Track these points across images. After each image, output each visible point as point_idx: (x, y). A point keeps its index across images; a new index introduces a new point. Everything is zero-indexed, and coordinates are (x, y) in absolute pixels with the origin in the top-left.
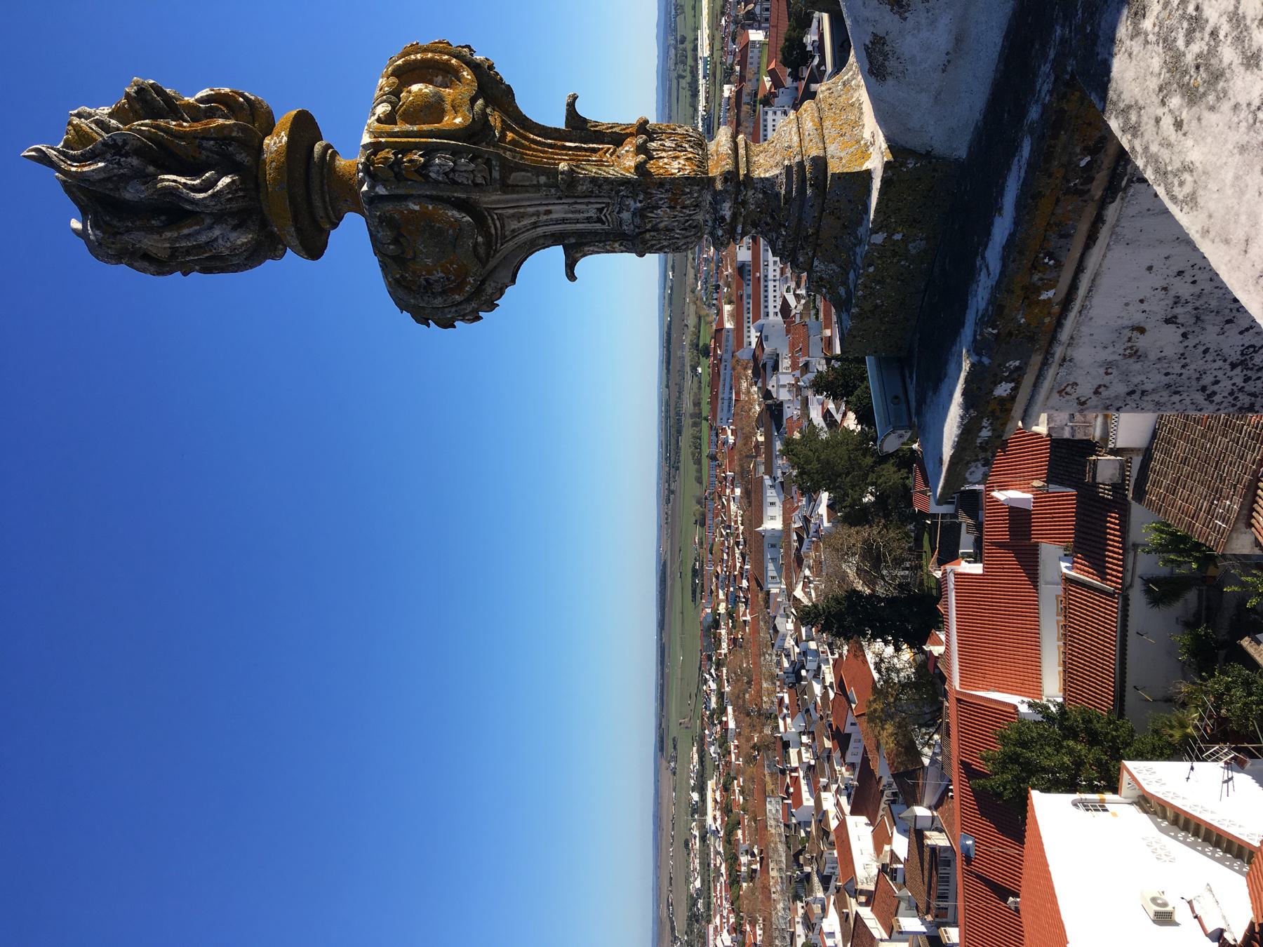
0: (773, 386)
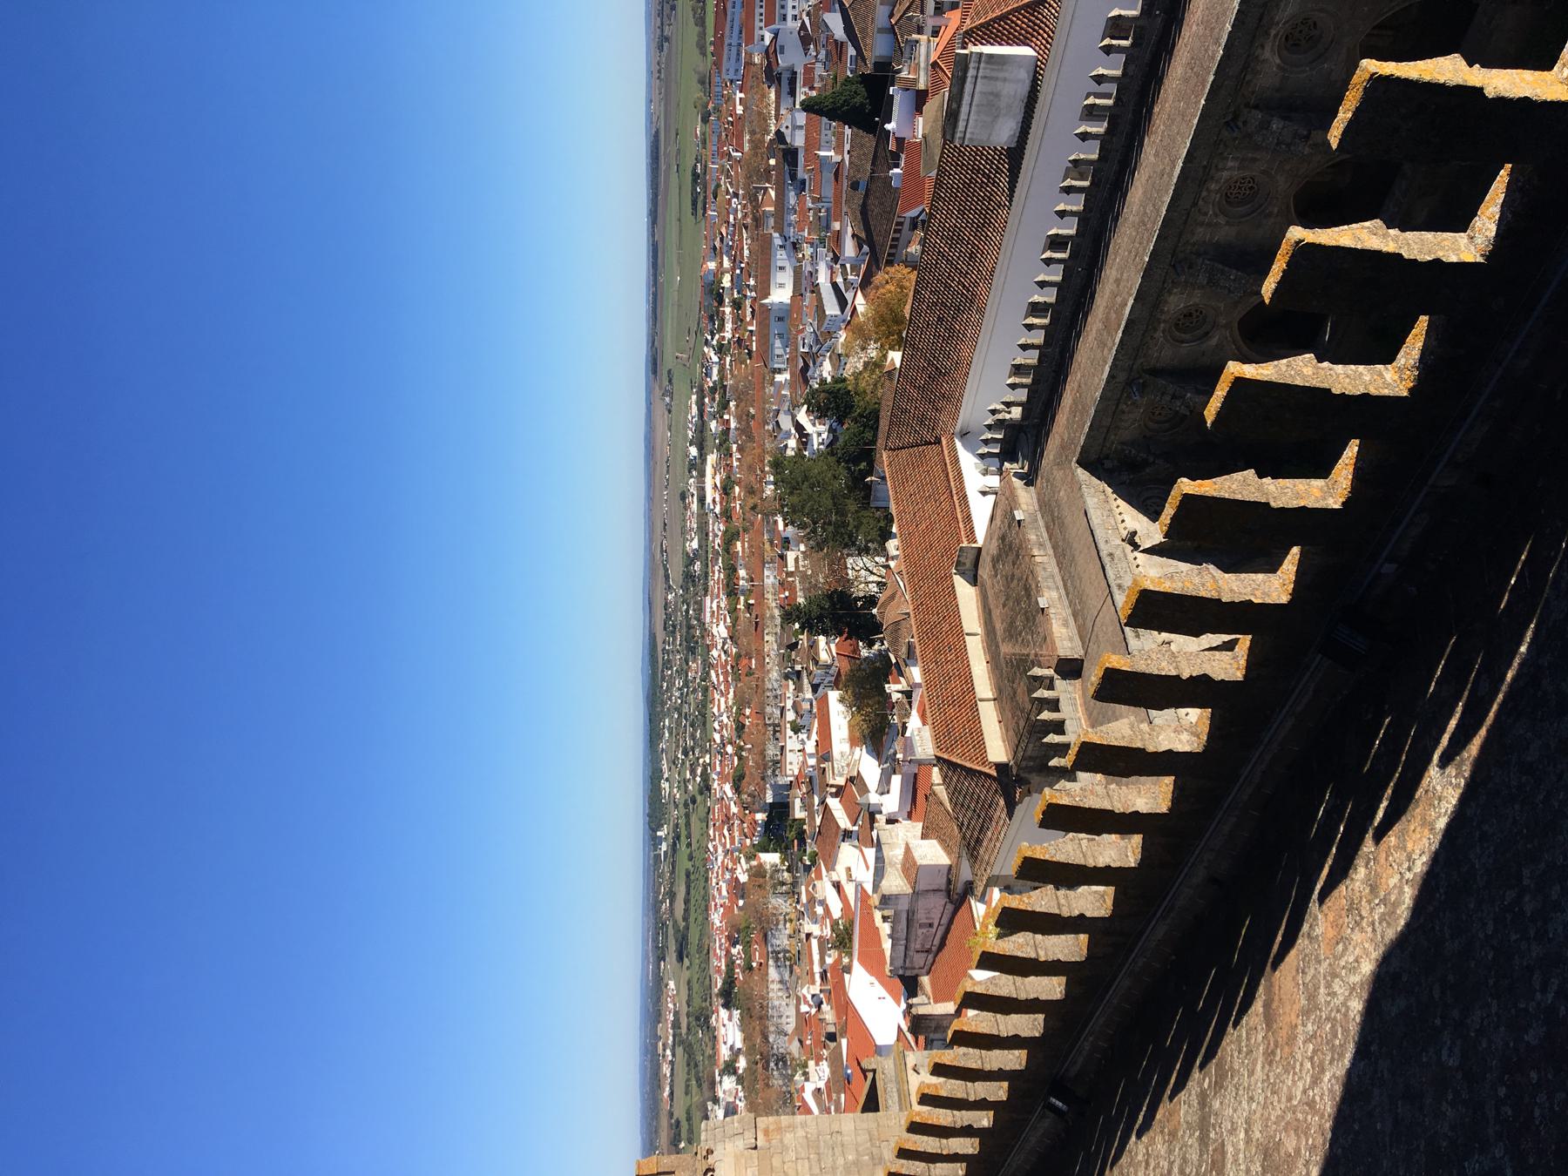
0: (787, 127)
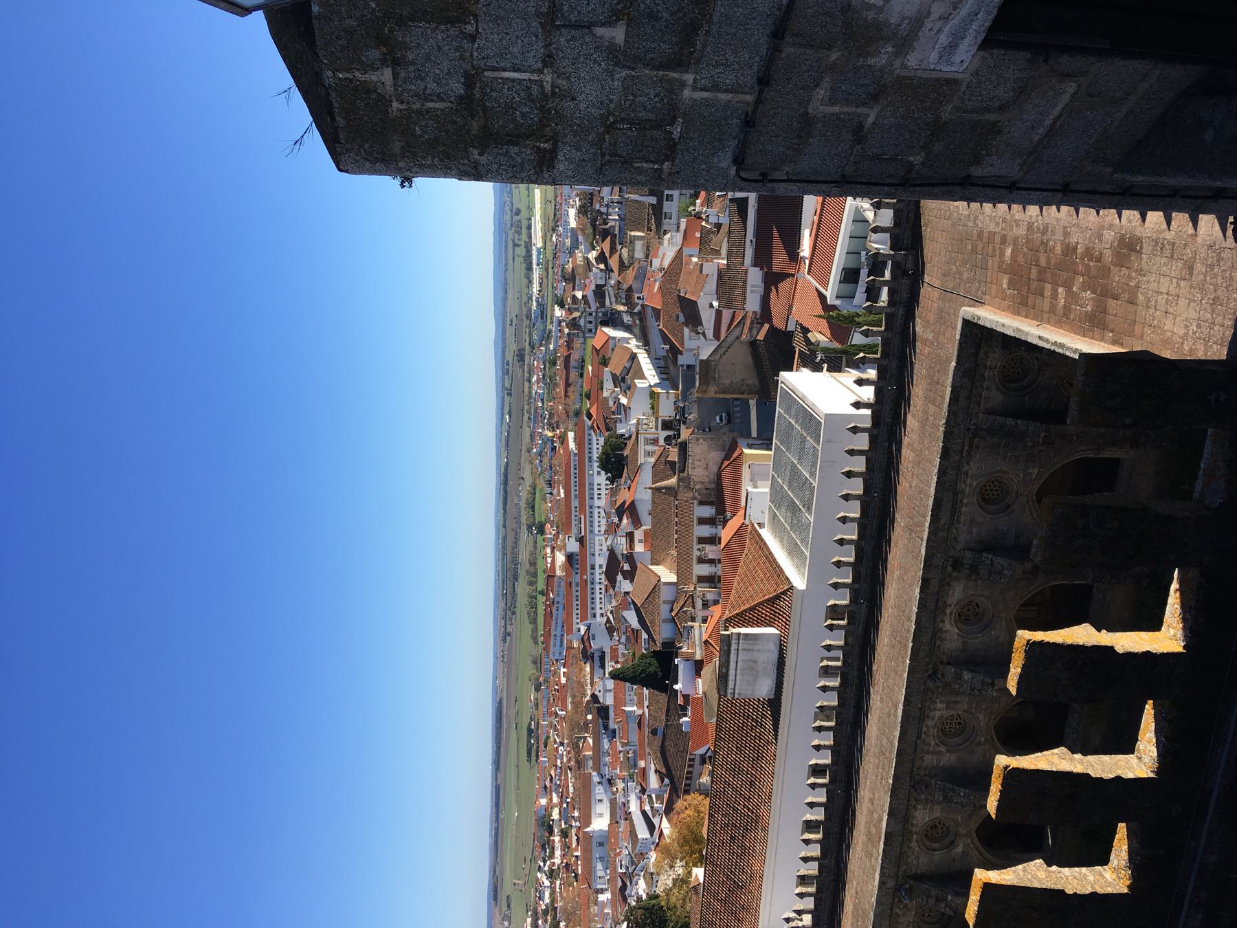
0: (600, 691)
